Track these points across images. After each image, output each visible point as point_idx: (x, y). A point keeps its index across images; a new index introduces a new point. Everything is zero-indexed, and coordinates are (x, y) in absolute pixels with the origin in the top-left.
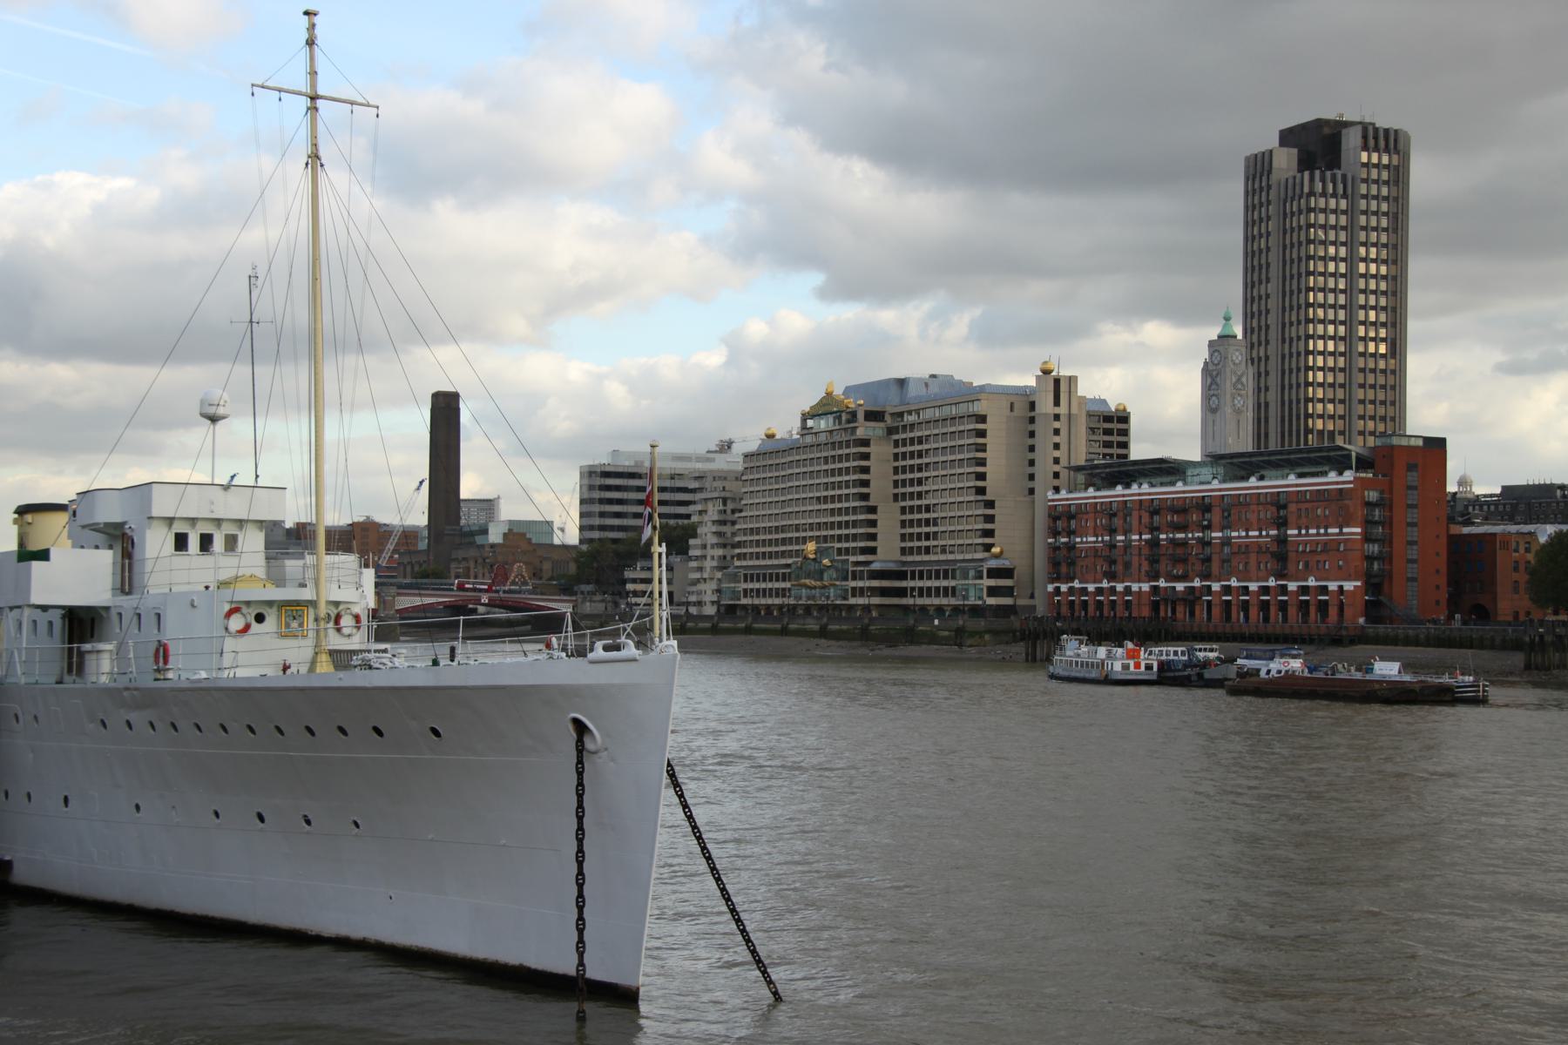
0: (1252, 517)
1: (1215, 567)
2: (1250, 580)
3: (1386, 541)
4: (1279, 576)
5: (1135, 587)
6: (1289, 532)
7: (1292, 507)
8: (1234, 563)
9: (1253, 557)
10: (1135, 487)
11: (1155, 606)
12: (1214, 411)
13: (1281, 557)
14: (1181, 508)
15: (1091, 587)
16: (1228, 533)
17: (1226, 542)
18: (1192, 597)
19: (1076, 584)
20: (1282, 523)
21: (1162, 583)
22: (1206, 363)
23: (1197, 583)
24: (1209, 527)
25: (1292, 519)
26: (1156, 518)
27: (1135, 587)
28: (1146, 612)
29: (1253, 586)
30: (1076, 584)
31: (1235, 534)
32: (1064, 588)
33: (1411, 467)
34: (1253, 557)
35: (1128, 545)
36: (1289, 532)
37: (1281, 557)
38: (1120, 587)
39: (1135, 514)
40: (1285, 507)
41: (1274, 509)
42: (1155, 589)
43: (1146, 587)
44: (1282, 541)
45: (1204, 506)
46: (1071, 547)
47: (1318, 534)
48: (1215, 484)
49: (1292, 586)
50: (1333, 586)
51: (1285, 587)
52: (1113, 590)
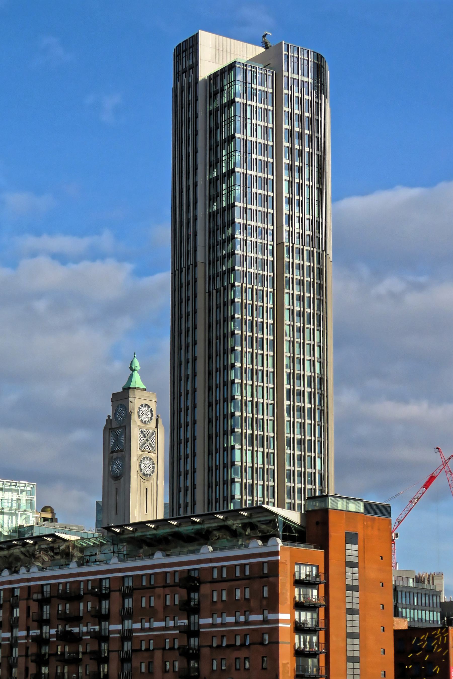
3: (324, 628)
6: (203, 621)
7: (205, 589)
8: (135, 663)
10: (23, 570)
14: (73, 596)
16: (128, 624)
17: (127, 636)
22: (109, 421)
24: (106, 617)
25: (205, 605)
26: (46, 609)
33: (351, 538)
34: (158, 654)
36: (203, 621)
39: (23, 604)
40: (196, 589)
41: (184, 592)
45: (99, 593)
48: (115, 563)
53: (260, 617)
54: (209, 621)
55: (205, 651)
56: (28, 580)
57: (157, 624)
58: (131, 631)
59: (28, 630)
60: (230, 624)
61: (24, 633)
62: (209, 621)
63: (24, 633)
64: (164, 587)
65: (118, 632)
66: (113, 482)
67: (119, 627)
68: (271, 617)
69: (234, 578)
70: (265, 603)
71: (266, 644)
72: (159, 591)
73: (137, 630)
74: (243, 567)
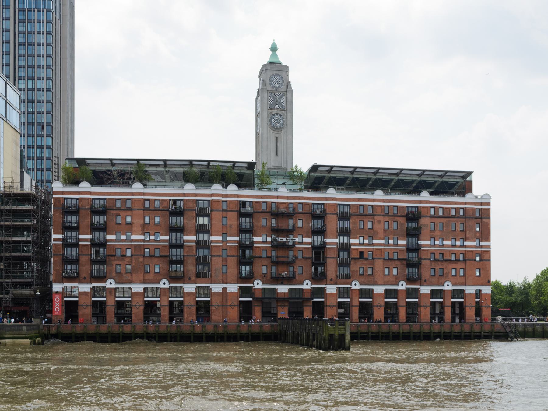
0: (379, 228)
2: (375, 283)
4: (410, 280)
5: (216, 288)
6: (423, 242)
7: (424, 221)
9: (379, 263)
11: (246, 311)
12: (277, 129)
13: (412, 264)
17: (342, 247)
18: (296, 301)
20: (414, 233)
21: (258, 285)
23: (307, 285)
27: (216, 288)
28: (234, 313)
29: (379, 289)
30: (110, 284)
31: (352, 241)
37: (412, 264)
38: (190, 288)
41: (402, 220)
42: (244, 292)
43: (233, 288)
47: (453, 246)
49: (425, 290)
50: (470, 290)
51: (418, 290)
53: (474, 243)
54: (428, 242)
55: (425, 263)
56: (222, 196)
57: (375, 241)
58: (349, 244)
59: (225, 234)
60: (448, 246)
61: (220, 238)
62: (428, 242)
63: (220, 238)
64: (384, 216)
65: (336, 244)
66: (271, 131)
67: (336, 241)
68: (482, 244)
69: (449, 215)
70: (478, 234)
71: (477, 261)
72: (381, 218)
73: (354, 244)
74: (457, 210)
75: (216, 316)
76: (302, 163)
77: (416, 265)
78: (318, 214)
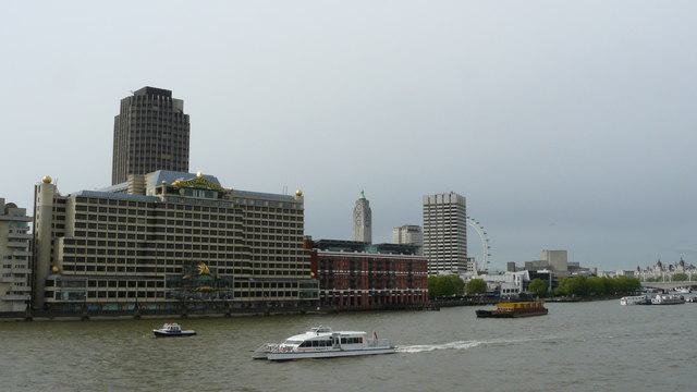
1: (391, 283)
5: (363, 291)
15: (342, 292)
18: (383, 296)
19: (334, 290)
20: (410, 270)
27: (363, 291)
30: (334, 290)
32: (327, 292)
35: (359, 274)
38: (356, 291)
44: (410, 275)
46: (331, 274)
52: (410, 292)
75: (363, 303)
76: (376, 240)
77: (410, 281)
78: (387, 261)
